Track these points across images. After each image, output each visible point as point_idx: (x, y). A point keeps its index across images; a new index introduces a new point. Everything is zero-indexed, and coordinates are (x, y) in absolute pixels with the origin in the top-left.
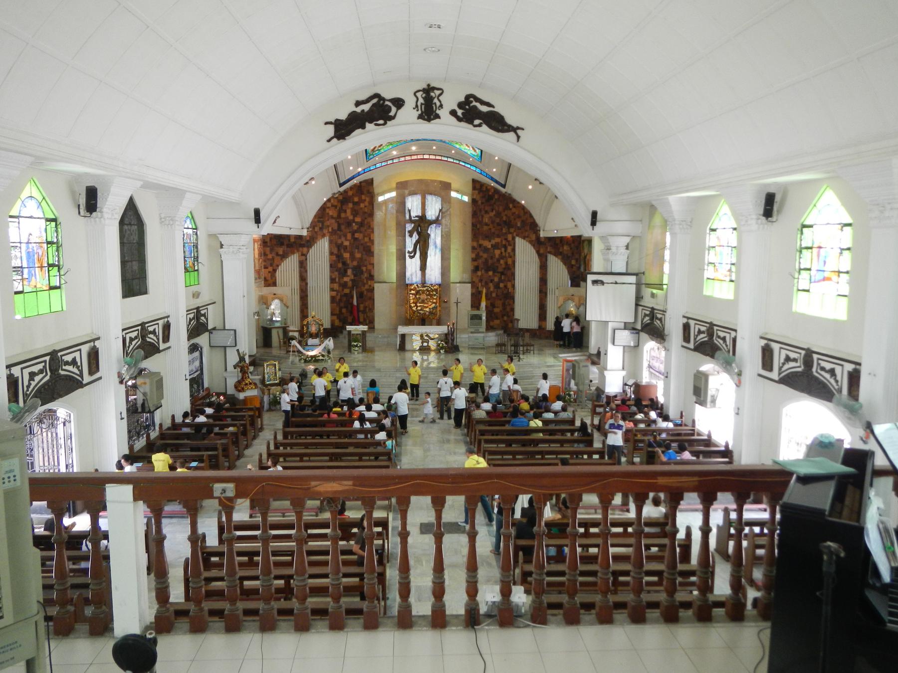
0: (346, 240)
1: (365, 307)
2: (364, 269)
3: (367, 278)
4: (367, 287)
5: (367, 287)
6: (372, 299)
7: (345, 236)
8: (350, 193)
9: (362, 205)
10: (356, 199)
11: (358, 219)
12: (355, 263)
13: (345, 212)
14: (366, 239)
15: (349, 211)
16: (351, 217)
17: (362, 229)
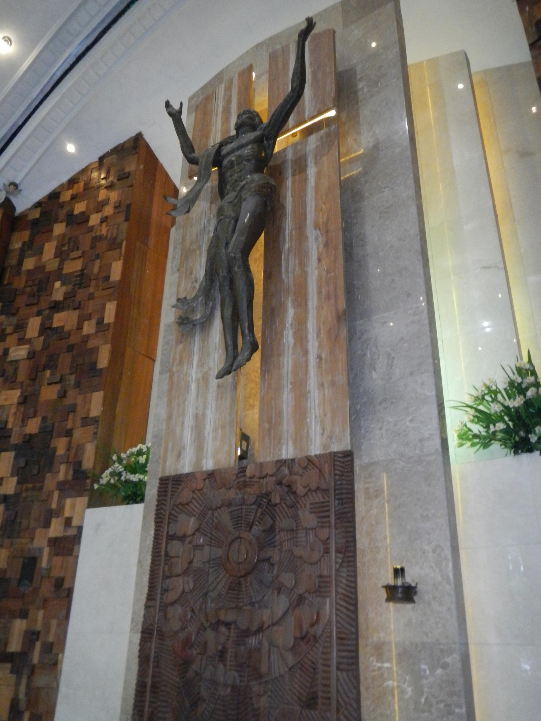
0: (22, 341)
1: (31, 637)
2: (60, 445)
3: (62, 487)
4: (56, 529)
5: (56, 529)
6: (63, 592)
7: (21, 327)
8: (66, 196)
9: (94, 219)
10: (80, 208)
11: (73, 267)
12: (33, 426)
13: (40, 252)
14: (89, 328)
15: (49, 249)
16: (52, 265)
17: (82, 294)
